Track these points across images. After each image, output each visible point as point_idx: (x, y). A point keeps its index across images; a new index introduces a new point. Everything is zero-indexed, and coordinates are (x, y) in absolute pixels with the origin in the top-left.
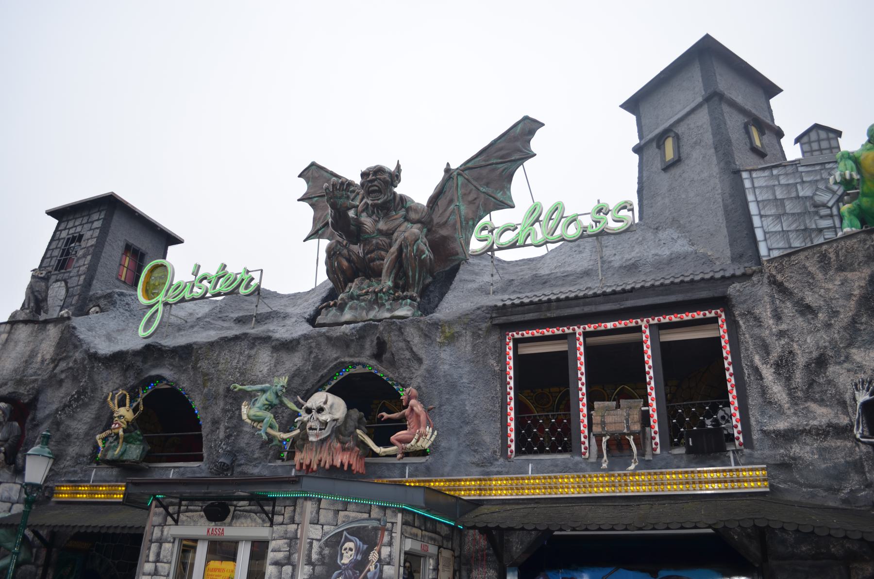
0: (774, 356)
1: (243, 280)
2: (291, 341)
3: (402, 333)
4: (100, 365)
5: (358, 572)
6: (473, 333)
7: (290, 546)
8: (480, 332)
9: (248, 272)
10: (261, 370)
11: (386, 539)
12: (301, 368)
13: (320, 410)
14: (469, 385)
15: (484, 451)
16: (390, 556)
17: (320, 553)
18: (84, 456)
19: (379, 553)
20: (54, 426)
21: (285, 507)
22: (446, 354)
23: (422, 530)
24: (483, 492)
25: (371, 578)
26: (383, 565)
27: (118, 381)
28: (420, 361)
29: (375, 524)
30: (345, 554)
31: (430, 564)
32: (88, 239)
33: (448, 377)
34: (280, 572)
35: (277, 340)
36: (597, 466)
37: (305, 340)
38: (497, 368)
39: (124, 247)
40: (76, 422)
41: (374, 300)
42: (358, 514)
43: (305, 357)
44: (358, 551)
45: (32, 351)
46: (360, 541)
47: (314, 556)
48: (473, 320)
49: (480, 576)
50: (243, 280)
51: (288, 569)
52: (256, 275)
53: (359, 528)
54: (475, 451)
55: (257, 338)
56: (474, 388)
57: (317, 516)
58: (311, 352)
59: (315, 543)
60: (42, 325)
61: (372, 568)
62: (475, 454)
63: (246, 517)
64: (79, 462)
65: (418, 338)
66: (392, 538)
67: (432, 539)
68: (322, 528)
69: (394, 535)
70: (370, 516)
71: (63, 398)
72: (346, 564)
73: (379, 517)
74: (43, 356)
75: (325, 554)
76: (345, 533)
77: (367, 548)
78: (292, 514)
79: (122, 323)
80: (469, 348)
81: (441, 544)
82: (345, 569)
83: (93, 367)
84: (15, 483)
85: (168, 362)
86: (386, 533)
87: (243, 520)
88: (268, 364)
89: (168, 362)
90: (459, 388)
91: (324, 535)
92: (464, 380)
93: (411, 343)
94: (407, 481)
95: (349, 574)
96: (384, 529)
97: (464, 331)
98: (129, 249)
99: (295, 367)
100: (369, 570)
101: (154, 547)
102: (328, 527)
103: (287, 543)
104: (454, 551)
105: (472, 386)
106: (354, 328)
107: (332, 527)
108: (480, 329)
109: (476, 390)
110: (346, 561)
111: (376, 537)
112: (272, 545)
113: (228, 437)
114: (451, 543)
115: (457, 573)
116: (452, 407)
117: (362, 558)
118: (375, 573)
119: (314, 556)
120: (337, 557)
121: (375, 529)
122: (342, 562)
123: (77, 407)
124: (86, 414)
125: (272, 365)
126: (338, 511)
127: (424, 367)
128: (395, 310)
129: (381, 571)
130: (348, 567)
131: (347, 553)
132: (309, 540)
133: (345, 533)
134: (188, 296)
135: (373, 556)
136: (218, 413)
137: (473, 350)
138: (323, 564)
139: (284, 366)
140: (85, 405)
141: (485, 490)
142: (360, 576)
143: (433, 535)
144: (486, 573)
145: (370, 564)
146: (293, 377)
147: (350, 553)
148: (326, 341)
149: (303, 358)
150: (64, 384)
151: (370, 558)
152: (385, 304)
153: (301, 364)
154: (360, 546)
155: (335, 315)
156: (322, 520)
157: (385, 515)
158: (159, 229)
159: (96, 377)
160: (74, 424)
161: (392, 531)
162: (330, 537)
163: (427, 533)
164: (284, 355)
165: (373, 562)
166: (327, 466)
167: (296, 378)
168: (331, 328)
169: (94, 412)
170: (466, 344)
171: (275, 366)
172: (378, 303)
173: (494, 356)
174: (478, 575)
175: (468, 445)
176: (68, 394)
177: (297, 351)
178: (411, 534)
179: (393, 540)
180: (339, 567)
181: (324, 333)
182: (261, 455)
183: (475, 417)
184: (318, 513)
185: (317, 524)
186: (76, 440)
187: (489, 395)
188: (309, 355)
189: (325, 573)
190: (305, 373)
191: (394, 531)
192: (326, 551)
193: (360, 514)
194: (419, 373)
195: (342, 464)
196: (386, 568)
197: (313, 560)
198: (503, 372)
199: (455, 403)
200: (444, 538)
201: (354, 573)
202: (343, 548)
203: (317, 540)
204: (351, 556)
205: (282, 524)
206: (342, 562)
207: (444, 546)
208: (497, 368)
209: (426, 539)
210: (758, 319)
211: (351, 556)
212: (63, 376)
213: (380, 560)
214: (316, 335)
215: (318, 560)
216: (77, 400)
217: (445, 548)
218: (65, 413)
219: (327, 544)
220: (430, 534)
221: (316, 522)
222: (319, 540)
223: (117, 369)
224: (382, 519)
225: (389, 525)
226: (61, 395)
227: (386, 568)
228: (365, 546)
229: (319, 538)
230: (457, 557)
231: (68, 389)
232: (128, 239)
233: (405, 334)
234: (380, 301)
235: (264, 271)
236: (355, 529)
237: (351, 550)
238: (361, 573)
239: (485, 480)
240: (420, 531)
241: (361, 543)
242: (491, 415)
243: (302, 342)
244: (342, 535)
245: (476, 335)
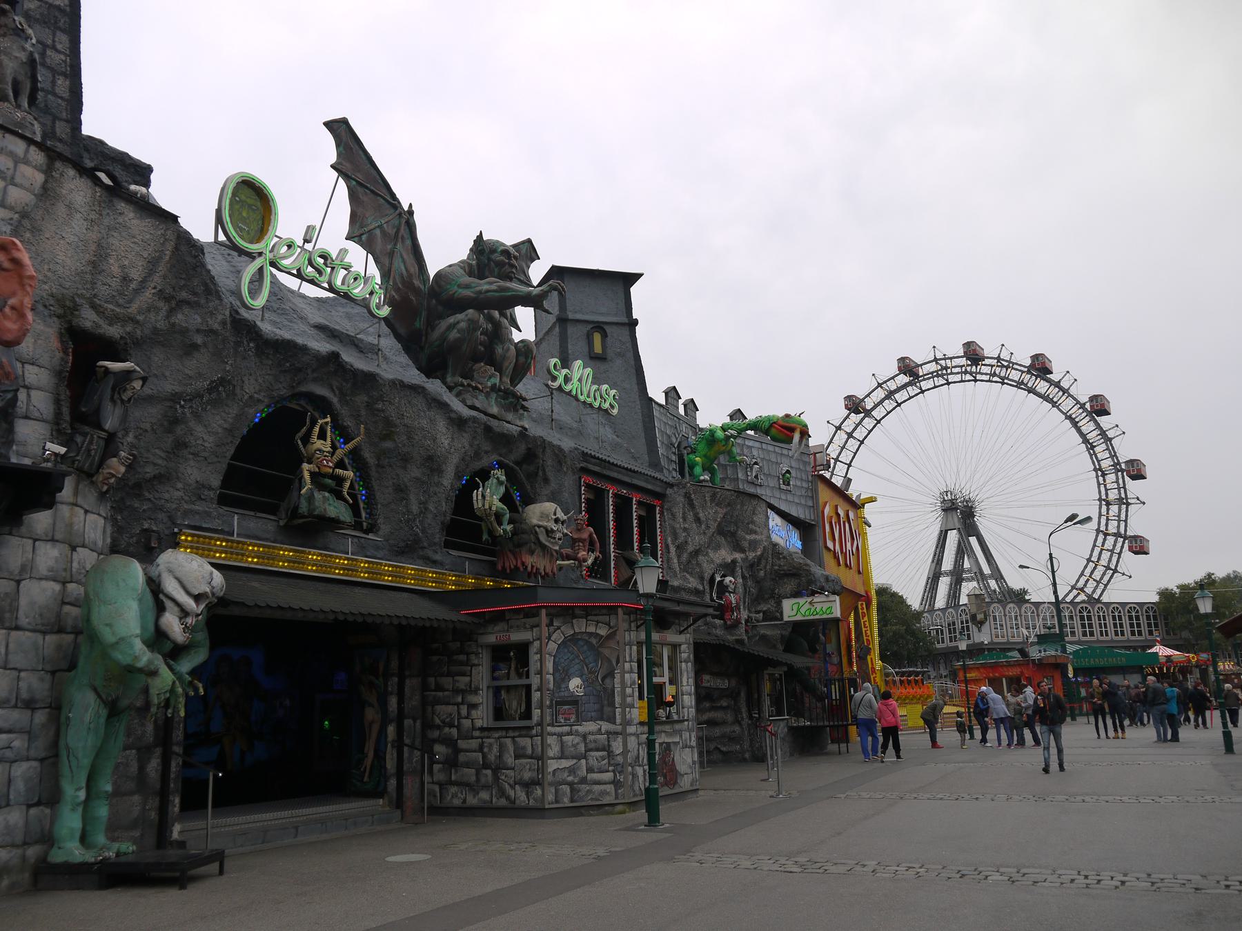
0: (677, 543)
4: (251, 345)
18: (210, 488)
55: (435, 399)
64: (202, 497)
84: (99, 514)
124: (218, 418)
160: (199, 430)
169: (230, 420)
186: (191, 456)
210: (673, 515)
212: (199, 340)
218: (191, 407)
223: (270, 362)
243: (470, 424)
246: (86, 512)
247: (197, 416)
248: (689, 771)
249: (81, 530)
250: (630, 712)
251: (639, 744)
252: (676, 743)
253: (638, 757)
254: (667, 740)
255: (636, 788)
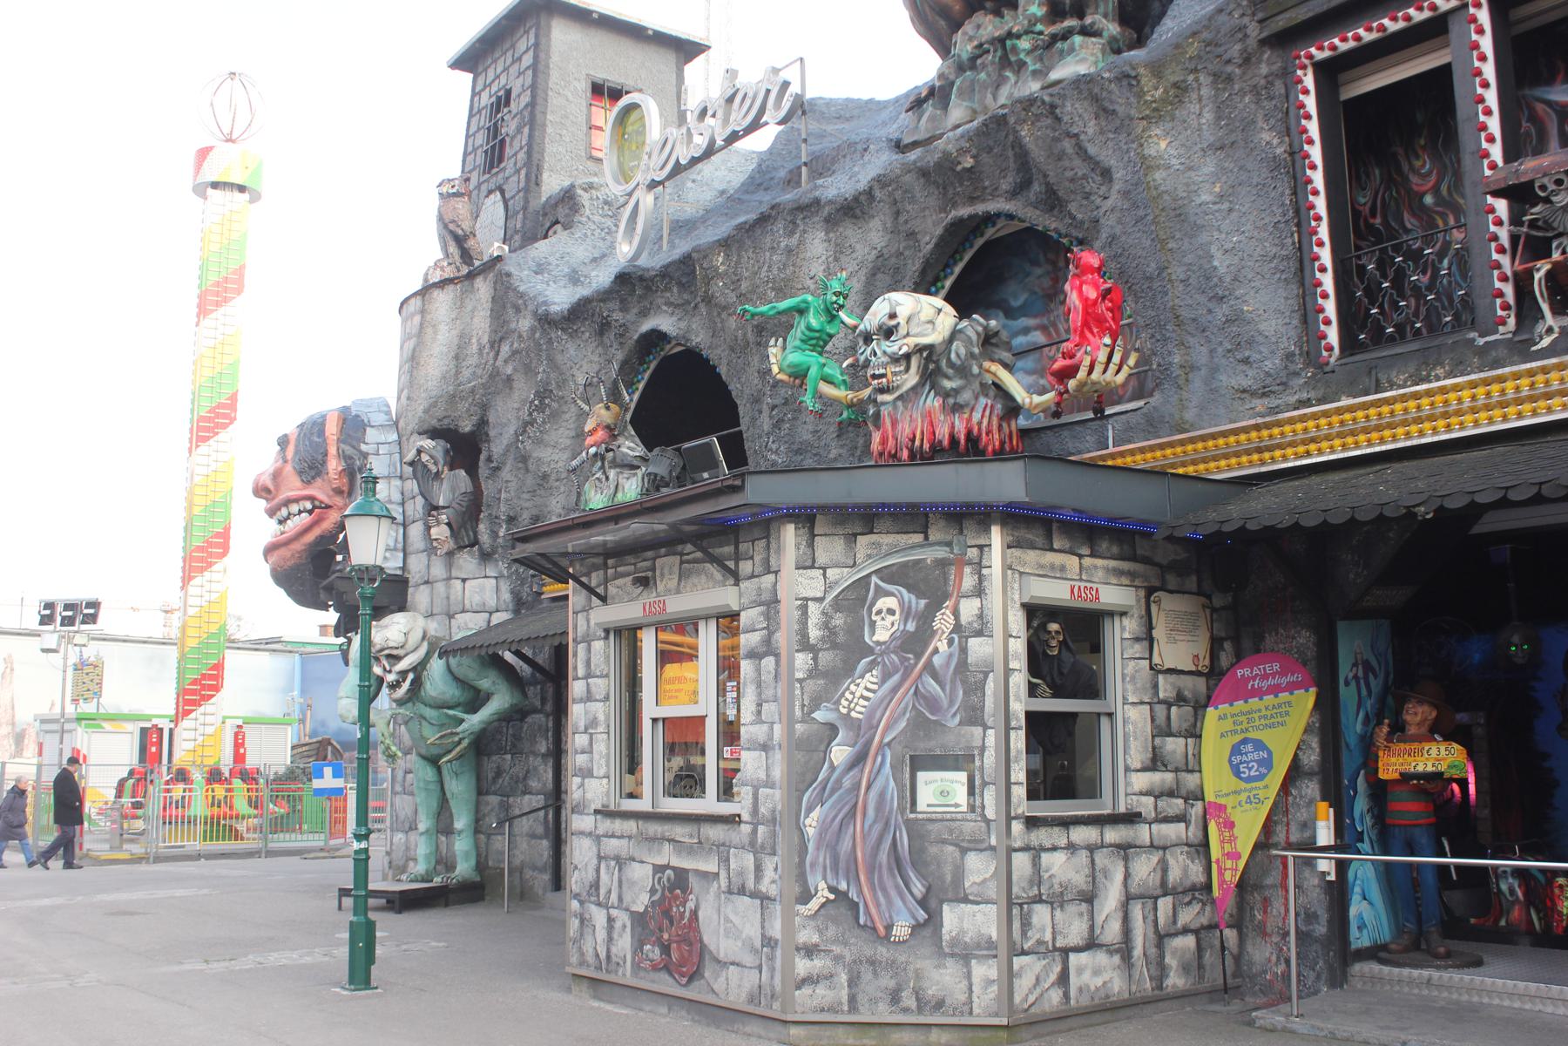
1: (768, 91)
2: (856, 199)
3: (1058, 119)
5: (911, 656)
6: (1214, 75)
7: (768, 618)
8: (1229, 69)
9: (776, 71)
10: (812, 274)
11: (969, 581)
12: (885, 251)
13: (888, 333)
14: (1216, 207)
15: (1266, 358)
16: (981, 616)
17: (825, 625)
19: (956, 613)
20: (520, 465)
21: (753, 542)
22: (1160, 144)
23: (1081, 556)
24: (1267, 455)
25: (941, 666)
26: (967, 637)
27: (596, 359)
28: (1106, 174)
29: (941, 553)
30: (879, 623)
31: (1123, 629)
32: (519, 96)
33: (1166, 197)
34: (758, 670)
35: (830, 202)
36: (1521, 348)
37: (882, 188)
38: (1279, 151)
39: (590, 90)
40: (550, 450)
41: (1000, 58)
42: (898, 537)
43: (889, 225)
44: (907, 614)
45: (461, 336)
46: (909, 592)
47: (814, 633)
48: (1209, 44)
49: (1281, 646)
50: (768, 91)
51: (769, 662)
52: (792, 75)
53: (905, 565)
54: (1246, 361)
56: (1230, 210)
57: (809, 552)
58: (898, 213)
59: (813, 608)
60: (466, 283)
61: (943, 646)
62: (1245, 368)
63: (699, 573)
65: (1093, 122)
66: (981, 578)
67: (1119, 573)
68: (824, 575)
69: (984, 571)
70: (926, 538)
71: (519, 409)
72: (885, 643)
73: (948, 538)
74: (479, 344)
75: (835, 627)
76: (874, 579)
77: (927, 606)
78: (764, 555)
79: (601, 244)
80: (1208, 116)
81: (1157, 583)
82: (882, 654)
83: (550, 341)
85: (663, 300)
86: (967, 570)
87: (695, 580)
88: (824, 258)
89: (663, 300)
90: (1192, 219)
91: (829, 587)
92: (1205, 197)
93: (1082, 137)
94: (1113, 456)
95: (892, 663)
96: (961, 562)
97: (1191, 77)
98: (604, 92)
99: (874, 252)
100: (936, 651)
101: (581, 648)
102: (837, 571)
103: (762, 613)
104: (1209, 597)
105: (1226, 206)
106: (962, 136)
107: (846, 570)
108: (1229, 62)
109: (1234, 215)
110: (882, 635)
111: (946, 580)
112: (745, 618)
113: (777, 425)
114: (1194, 578)
115: (1227, 645)
116: (1185, 268)
117: (917, 628)
118: (950, 656)
119: (814, 633)
120: (863, 630)
121: (942, 564)
122: (875, 639)
123: (544, 422)
124: (560, 431)
125: (831, 259)
126: (855, 535)
127: (1117, 187)
128: (1049, 69)
129: (964, 650)
130: (888, 648)
131: (883, 619)
132: (799, 602)
133: (874, 579)
134: (683, 153)
135: (943, 621)
136: (756, 382)
137: (1219, 118)
138: (835, 646)
139: (854, 255)
140: (555, 416)
141: (1270, 449)
142: (916, 664)
143: (1125, 565)
144: (1294, 638)
145: (937, 637)
146: (874, 275)
147: (890, 618)
148: (922, 180)
149: (885, 229)
150: (516, 385)
151: (936, 625)
152: (1025, 63)
153: (883, 244)
154: (910, 602)
155: (932, 119)
156: (822, 558)
157: (961, 532)
158: (650, 32)
159: (559, 358)
161: (980, 564)
162: (843, 590)
163: (1099, 562)
164: (849, 232)
165: (943, 632)
166: (926, 446)
167: (880, 276)
168: (928, 148)
170: (1201, 109)
171: (836, 260)
172: (1010, 64)
173: (1272, 121)
174: (1276, 643)
175: (1229, 351)
176: (524, 402)
177: (873, 217)
178: (1042, 566)
179: (985, 583)
180: (870, 651)
181: (915, 162)
182: (841, 451)
183: (1235, 279)
184: (811, 545)
185: (812, 567)
187: (1267, 221)
188: (896, 219)
189: (839, 664)
190: (893, 260)
191: (984, 563)
192: (839, 620)
193: (904, 536)
194: (1109, 203)
195: (953, 440)
196: (973, 642)
197: (812, 641)
198: (1296, 156)
199: (1189, 258)
200: (1164, 569)
201: (903, 660)
202: (874, 612)
203: (815, 599)
204: (893, 624)
205: (753, 576)
206: (875, 639)
207: (1170, 587)
208: (1279, 151)
209: (1100, 574)
211: (893, 624)
213: (958, 628)
214: (898, 171)
215: (823, 639)
216: (541, 408)
217: (1171, 592)
219: (837, 605)
220: (1112, 563)
221: (809, 563)
222: (820, 600)
224: (955, 541)
225: (973, 553)
226: (516, 405)
227: (973, 642)
228: (923, 602)
229: (819, 595)
230: (1223, 608)
231: (524, 390)
232: (592, 73)
233: (1066, 118)
234: (1013, 59)
235: (806, 62)
236: (894, 568)
237: (891, 612)
238: (918, 656)
239: (1268, 426)
240: (1076, 559)
241: (913, 598)
242: (1275, 268)
243: (878, 194)
244: (869, 584)
245: (1222, 79)
246: (464, 580)
247: (539, 442)
248: (748, 959)
249: (460, 598)
250: (582, 785)
251: (600, 858)
252: (705, 876)
253: (596, 885)
254: (676, 862)
255: (588, 948)
